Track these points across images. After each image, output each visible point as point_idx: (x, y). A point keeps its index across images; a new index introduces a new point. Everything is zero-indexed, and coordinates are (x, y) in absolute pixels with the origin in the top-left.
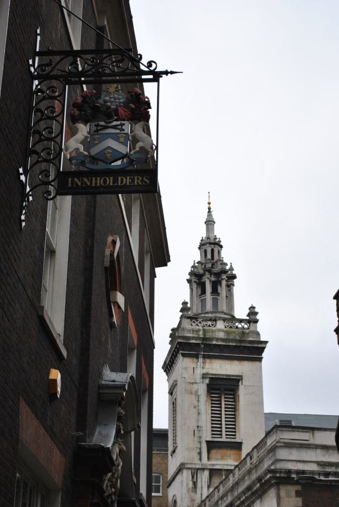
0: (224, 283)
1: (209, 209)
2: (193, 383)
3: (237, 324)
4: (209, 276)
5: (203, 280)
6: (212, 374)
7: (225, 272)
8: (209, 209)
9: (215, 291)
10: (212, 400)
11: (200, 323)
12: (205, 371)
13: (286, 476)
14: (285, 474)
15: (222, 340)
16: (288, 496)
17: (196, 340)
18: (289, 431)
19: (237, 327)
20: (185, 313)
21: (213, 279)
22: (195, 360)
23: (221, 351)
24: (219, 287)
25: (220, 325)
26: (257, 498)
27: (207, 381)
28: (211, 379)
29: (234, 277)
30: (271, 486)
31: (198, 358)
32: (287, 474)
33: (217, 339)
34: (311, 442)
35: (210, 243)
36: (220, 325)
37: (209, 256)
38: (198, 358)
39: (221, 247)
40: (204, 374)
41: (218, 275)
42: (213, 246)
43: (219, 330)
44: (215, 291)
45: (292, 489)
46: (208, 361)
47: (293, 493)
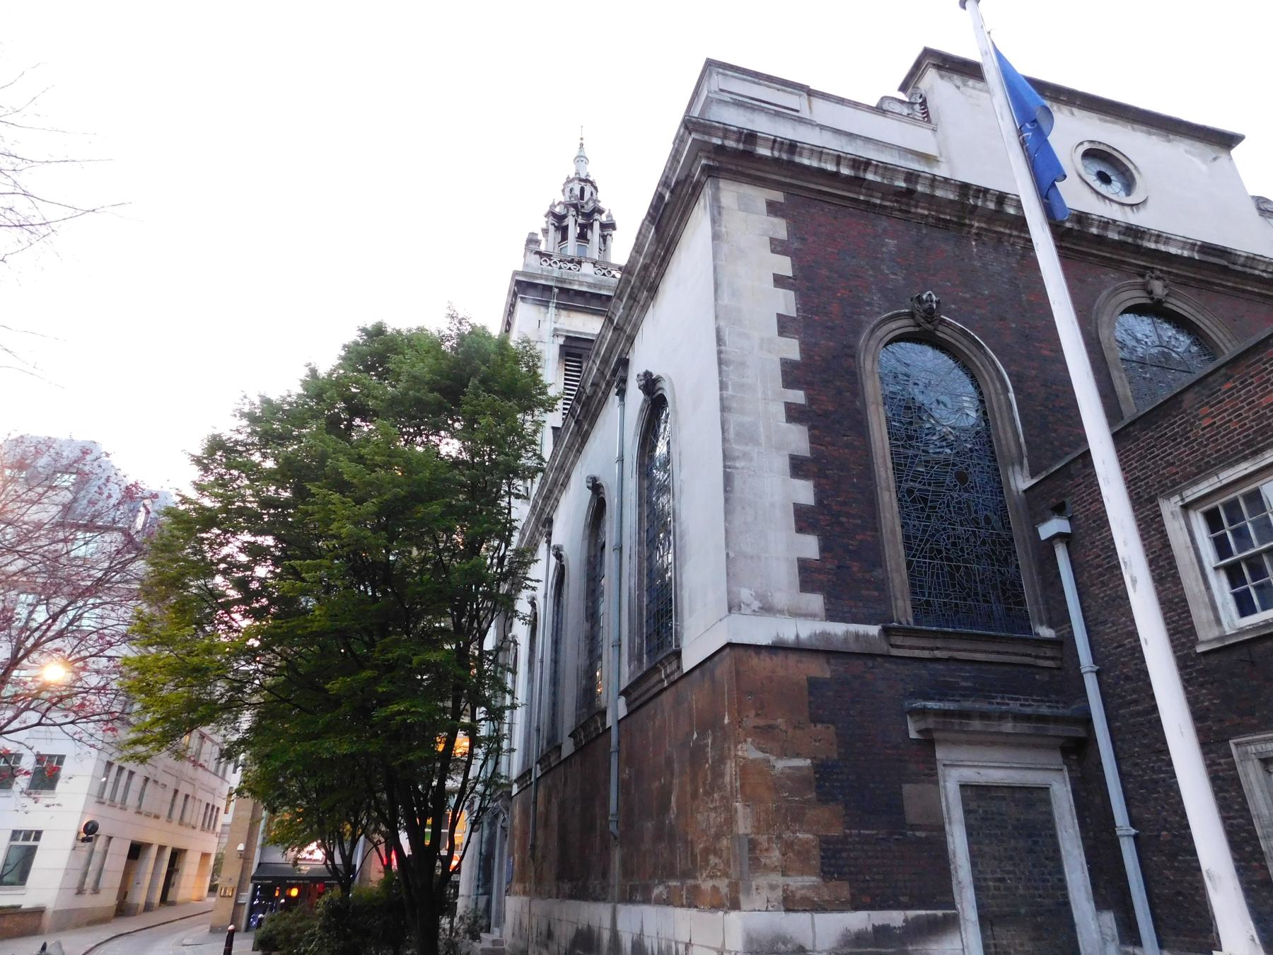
0: (596, 226)
1: (582, 145)
3: (613, 272)
4: (574, 213)
5: (564, 224)
6: (568, 331)
7: (601, 212)
8: (582, 145)
9: (582, 237)
10: (566, 370)
11: (555, 263)
12: (557, 326)
13: (741, 146)
14: (738, 141)
15: (590, 285)
16: (745, 207)
17: (546, 279)
18: (744, 80)
19: (614, 276)
20: (532, 246)
21: (580, 220)
22: (543, 309)
23: (587, 302)
24: (589, 232)
25: (587, 268)
26: (645, 308)
27: (561, 341)
28: (567, 337)
29: (611, 226)
30: (697, 189)
31: (548, 307)
32: (744, 143)
33: (581, 283)
34: (805, 114)
35: (581, 180)
36: (587, 268)
37: (577, 192)
38: (546, 304)
39: (596, 188)
40: (556, 329)
41: (589, 216)
42: (583, 184)
43: (585, 275)
44: (582, 237)
45: (760, 196)
46: (563, 313)
47: (763, 207)
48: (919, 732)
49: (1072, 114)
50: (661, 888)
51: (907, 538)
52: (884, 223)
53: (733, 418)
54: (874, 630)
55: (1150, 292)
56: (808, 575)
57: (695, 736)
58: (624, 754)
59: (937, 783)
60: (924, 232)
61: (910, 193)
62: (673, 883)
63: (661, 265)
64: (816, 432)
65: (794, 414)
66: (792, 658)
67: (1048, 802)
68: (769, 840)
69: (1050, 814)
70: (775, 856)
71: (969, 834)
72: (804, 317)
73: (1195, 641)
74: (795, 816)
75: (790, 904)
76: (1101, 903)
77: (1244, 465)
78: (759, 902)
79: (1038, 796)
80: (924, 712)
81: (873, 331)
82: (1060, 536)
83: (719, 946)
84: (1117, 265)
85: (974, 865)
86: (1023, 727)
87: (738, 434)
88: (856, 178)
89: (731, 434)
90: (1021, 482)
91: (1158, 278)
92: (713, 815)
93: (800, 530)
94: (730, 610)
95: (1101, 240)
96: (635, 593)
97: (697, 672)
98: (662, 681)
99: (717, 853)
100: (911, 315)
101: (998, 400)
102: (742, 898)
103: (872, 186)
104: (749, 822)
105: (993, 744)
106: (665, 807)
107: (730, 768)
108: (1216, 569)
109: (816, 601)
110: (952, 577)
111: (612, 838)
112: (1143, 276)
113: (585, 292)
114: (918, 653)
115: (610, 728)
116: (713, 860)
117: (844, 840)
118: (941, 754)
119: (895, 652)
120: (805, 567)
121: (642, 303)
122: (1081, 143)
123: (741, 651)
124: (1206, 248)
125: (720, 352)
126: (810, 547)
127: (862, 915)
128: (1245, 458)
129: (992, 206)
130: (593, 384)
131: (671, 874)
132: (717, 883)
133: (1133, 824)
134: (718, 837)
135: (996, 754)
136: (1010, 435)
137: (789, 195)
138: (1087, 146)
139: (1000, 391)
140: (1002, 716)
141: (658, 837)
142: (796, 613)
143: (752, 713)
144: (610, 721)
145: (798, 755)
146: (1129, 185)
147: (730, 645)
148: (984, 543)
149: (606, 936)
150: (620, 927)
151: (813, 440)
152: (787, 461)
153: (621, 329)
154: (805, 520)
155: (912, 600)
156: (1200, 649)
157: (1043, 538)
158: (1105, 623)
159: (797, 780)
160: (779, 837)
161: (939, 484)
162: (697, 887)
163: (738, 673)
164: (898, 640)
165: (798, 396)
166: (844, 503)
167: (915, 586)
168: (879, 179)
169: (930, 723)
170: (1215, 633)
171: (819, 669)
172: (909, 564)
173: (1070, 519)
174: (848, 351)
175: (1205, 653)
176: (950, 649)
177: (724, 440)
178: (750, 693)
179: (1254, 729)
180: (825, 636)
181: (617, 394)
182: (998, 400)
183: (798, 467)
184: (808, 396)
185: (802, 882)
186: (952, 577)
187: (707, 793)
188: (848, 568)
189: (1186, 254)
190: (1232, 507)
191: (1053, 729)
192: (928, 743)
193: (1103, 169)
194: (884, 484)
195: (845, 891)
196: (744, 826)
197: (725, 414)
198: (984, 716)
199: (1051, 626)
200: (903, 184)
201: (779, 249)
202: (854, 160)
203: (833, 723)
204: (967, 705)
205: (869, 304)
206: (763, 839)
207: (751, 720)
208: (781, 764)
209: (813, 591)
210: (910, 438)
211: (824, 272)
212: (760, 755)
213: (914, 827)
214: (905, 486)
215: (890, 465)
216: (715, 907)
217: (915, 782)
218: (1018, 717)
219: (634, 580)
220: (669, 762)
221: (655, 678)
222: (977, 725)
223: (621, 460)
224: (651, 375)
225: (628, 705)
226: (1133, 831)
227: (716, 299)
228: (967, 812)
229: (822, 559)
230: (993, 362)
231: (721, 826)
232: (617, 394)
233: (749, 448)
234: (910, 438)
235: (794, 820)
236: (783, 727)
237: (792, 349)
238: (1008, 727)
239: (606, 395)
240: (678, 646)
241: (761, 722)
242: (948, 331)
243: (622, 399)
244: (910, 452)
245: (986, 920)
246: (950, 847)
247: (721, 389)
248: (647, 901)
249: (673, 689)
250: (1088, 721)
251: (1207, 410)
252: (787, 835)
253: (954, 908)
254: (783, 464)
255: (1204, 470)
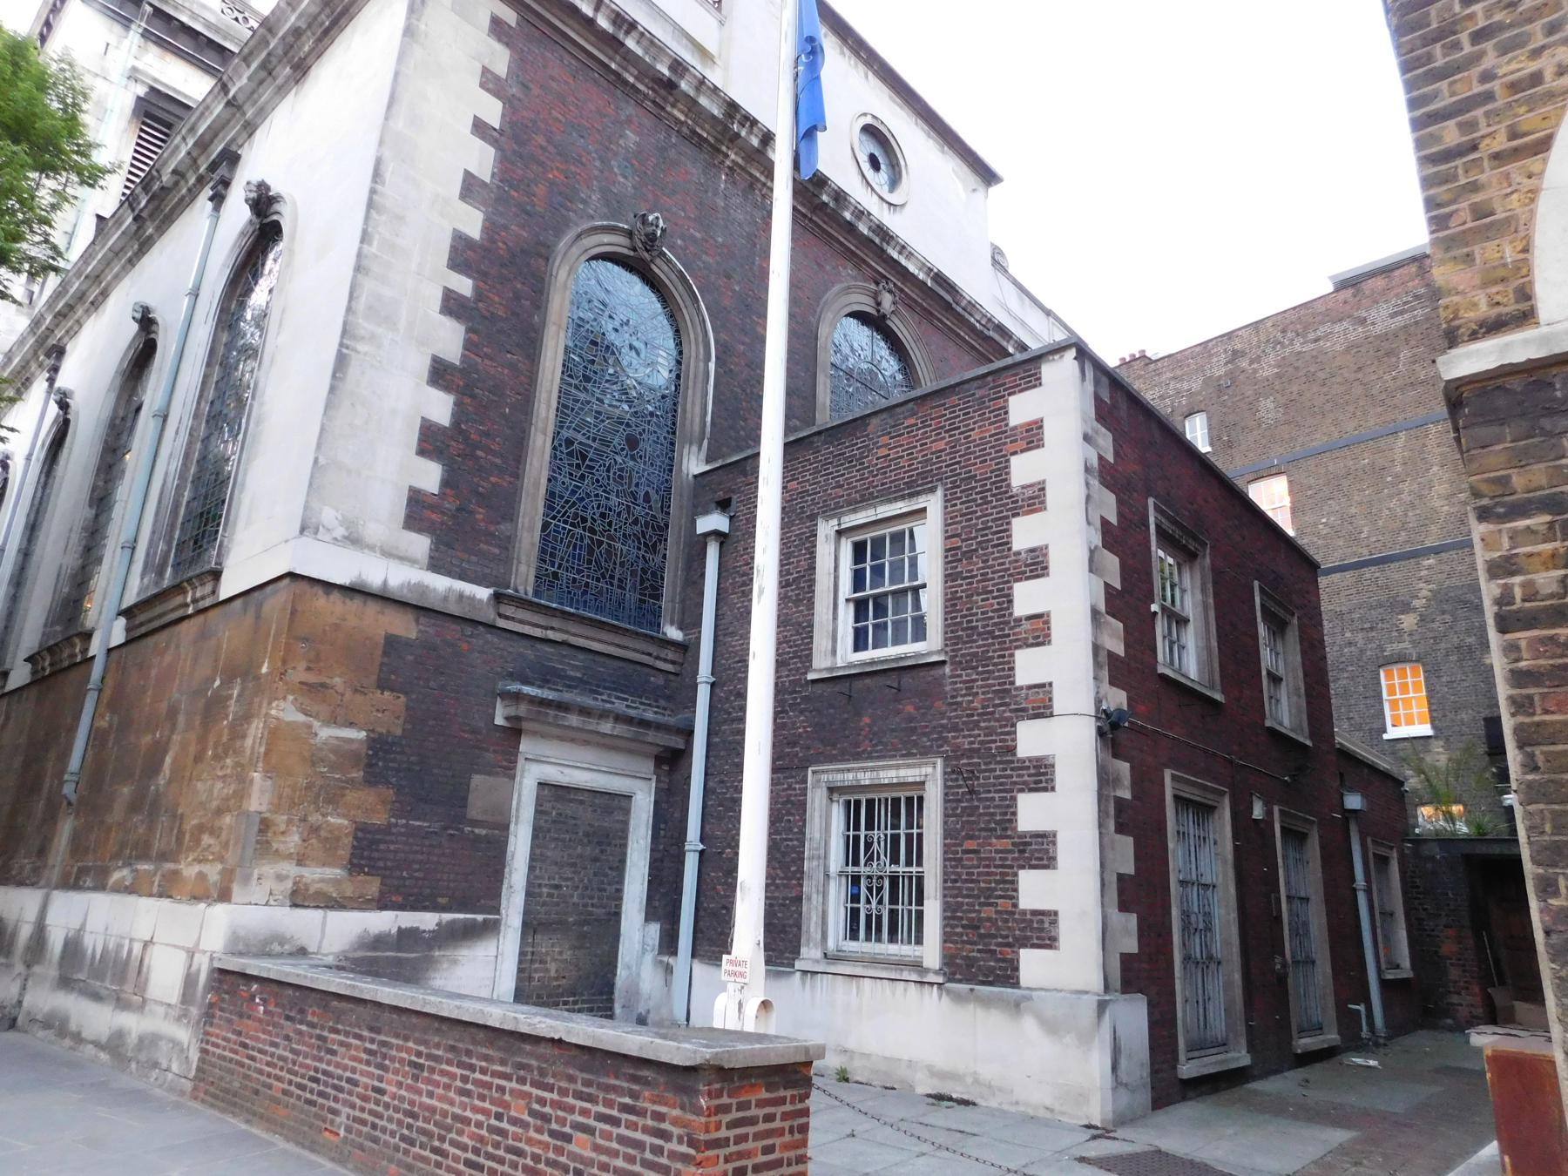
2: (97, 75)
6: (155, 80)
15: (208, 25)
23: (199, 49)
26: (282, 91)
27: (141, 91)
28: (152, 89)
31: (127, 28)
33: (194, 16)
38: (127, 28)
40: (134, 69)
46: (154, 50)
48: (507, 718)
49: (867, 77)
50: (125, 872)
51: (551, 495)
52: (630, 110)
53: (368, 285)
54: (483, 593)
55: (879, 304)
56: (418, 511)
57: (217, 683)
58: (107, 693)
59: (513, 777)
60: (673, 140)
61: (671, 86)
62: (144, 867)
63: (320, 40)
64: (474, 337)
65: (452, 305)
66: (372, 607)
67: (627, 812)
68: (289, 822)
69: (626, 823)
70: (293, 841)
71: (535, 837)
72: (498, 187)
73: (809, 668)
74: (331, 796)
75: (299, 898)
76: (651, 915)
77: (900, 504)
78: (258, 892)
79: (618, 803)
80: (517, 697)
81: (579, 236)
82: (716, 534)
83: (191, 945)
84: (858, 262)
85: (531, 868)
86: (621, 729)
87: (370, 308)
88: (614, 38)
89: (361, 304)
90: (694, 464)
91: (890, 291)
92: (219, 785)
93: (422, 452)
94: (302, 530)
95: (850, 228)
96: (173, 483)
97: (238, 603)
98: (187, 605)
99: (214, 832)
100: (630, 234)
101: (696, 367)
102: (236, 889)
103: (629, 57)
104: (267, 798)
105: (586, 743)
106: (153, 768)
107: (256, 729)
108: (848, 600)
109: (421, 544)
110: (591, 552)
111: (65, 803)
112: (877, 284)
113: (198, 33)
114: (527, 630)
115: (93, 657)
116: (207, 839)
117: (387, 829)
118: (526, 746)
119: (501, 623)
120: (416, 500)
121: (280, 81)
122: (865, 114)
123: (304, 586)
124: (940, 278)
125: (373, 191)
126: (430, 476)
127: (388, 916)
128: (903, 498)
129: (755, 142)
130: (174, 172)
131: (144, 856)
132: (206, 868)
133: (702, 840)
134: (219, 812)
135: (587, 755)
136: (697, 410)
137: (522, 19)
138: (869, 120)
139: (701, 357)
140: (603, 715)
141: (134, 807)
142: (388, 553)
143: (302, 665)
144: (96, 647)
145: (351, 725)
146: (895, 182)
147: (291, 575)
148: (636, 522)
149: (25, 932)
150: (49, 921)
151: (469, 346)
152: (427, 362)
153: (239, 108)
154: (431, 441)
155: (539, 568)
156: (811, 676)
157: (699, 531)
158: (732, 634)
159: (343, 755)
160: (304, 820)
161: (605, 442)
162: (176, 873)
163: (294, 612)
164: (509, 610)
165: (464, 285)
166: (487, 434)
167: (546, 552)
168: (639, 52)
169: (522, 709)
170: (827, 663)
171: (404, 626)
172: (545, 526)
173: (731, 518)
174: (543, 251)
175: (814, 681)
176: (567, 632)
177: (349, 309)
178: (305, 640)
179: (832, 759)
180: (422, 589)
181: (211, 199)
182: (696, 367)
183: (440, 374)
184: (476, 288)
185: (319, 875)
186: (591, 552)
187: (216, 757)
188: (472, 512)
189: (921, 276)
190: (878, 543)
191: (652, 736)
192: (514, 732)
193: (877, 154)
194: (540, 425)
195: (373, 887)
196: (259, 799)
197: (359, 276)
198: (585, 712)
199: (681, 629)
200: (666, 72)
201: (491, 86)
202: (618, 14)
203: (406, 693)
204: (567, 696)
205: (584, 202)
206: (281, 819)
207: (298, 674)
208: (326, 733)
209: (419, 531)
210: (587, 379)
211: (541, 140)
212: (301, 718)
213: (475, 823)
214: (565, 434)
215: (554, 405)
216: (196, 898)
217: (489, 774)
218: (619, 718)
219: (176, 465)
220: (173, 713)
221: (178, 600)
222: (574, 720)
223: (195, 294)
224: (268, 188)
225: (128, 630)
226: (701, 847)
227: (386, 119)
228: (539, 812)
229: (442, 495)
230: (704, 321)
231: (227, 799)
232: (211, 199)
233: (380, 331)
234: (587, 379)
235: (329, 801)
236: (340, 688)
237: (472, 223)
238: (607, 727)
239: (193, 195)
240: (219, 563)
241: (312, 678)
242: (665, 268)
243: (217, 208)
244: (582, 396)
245: (530, 927)
246: (511, 848)
247: (362, 241)
248: (100, 887)
249: (201, 618)
250: (689, 733)
251: (885, 440)
252: (315, 818)
253: (498, 912)
254: (423, 366)
255: (866, 499)
